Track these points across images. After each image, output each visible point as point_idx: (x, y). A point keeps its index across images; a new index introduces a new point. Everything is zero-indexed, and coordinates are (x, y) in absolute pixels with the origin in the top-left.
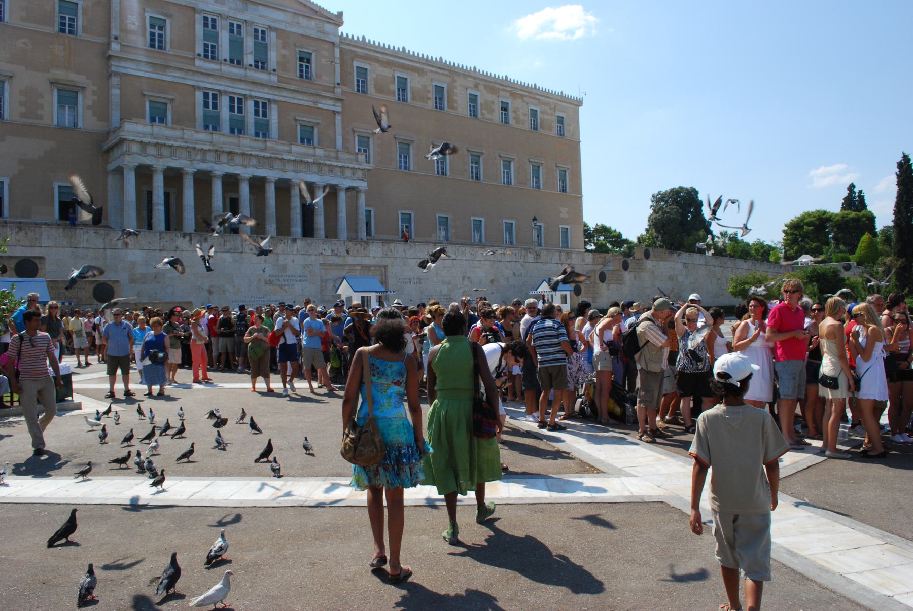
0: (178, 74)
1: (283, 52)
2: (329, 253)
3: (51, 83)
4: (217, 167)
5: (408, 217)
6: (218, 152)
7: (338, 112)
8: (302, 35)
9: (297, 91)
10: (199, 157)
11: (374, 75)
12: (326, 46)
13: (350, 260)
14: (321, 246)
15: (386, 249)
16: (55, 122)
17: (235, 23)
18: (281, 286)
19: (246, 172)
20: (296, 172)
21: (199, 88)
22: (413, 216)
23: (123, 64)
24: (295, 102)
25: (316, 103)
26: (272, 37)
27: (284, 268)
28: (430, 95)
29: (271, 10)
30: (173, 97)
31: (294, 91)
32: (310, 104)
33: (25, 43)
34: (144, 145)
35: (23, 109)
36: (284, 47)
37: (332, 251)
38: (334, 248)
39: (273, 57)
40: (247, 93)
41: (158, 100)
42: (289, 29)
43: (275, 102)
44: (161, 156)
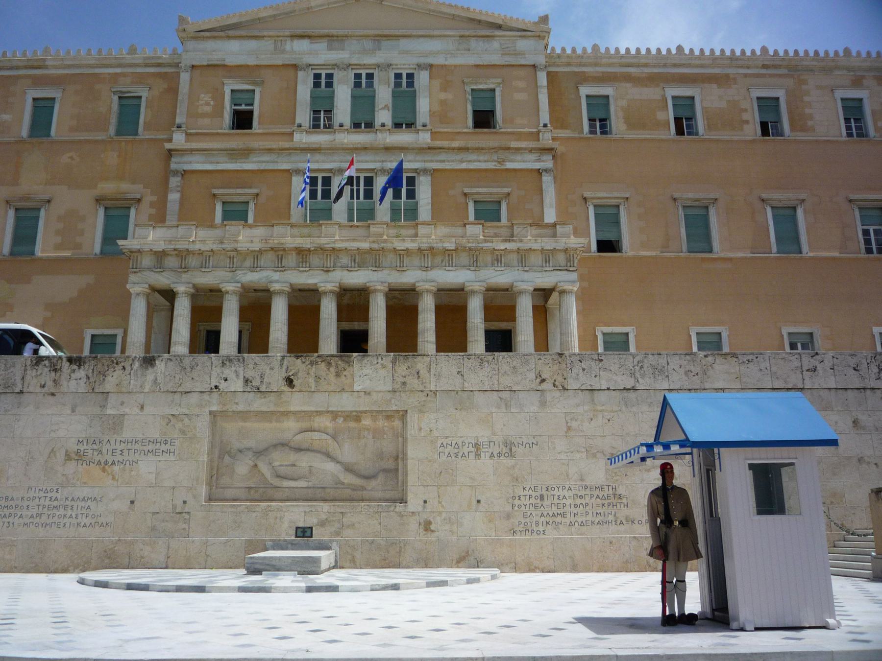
0: (266, 158)
1: (442, 96)
2: (237, 385)
3: (97, 200)
4: (276, 276)
5: (714, 339)
6: (280, 253)
7: (546, 171)
8: (477, 66)
9: (465, 149)
10: (248, 263)
11: (623, 103)
12: (522, 72)
13: (296, 401)
14: (216, 371)
15: (402, 369)
16: (97, 249)
17: (364, 73)
18: (104, 466)
19: (327, 281)
20: (426, 269)
21: (298, 172)
22: (725, 335)
23: (186, 159)
24: (464, 166)
25: (501, 162)
26: (422, 79)
27: (117, 423)
28: (746, 116)
29: (421, 40)
30: (255, 191)
31: (460, 149)
32: (491, 166)
33: (72, 158)
34: (160, 256)
35: (59, 239)
36: (444, 88)
37: (247, 381)
38: (250, 374)
39: (424, 106)
40: (377, 165)
41: (236, 199)
42: (451, 61)
43: (425, 171)
44: (185, 269)
